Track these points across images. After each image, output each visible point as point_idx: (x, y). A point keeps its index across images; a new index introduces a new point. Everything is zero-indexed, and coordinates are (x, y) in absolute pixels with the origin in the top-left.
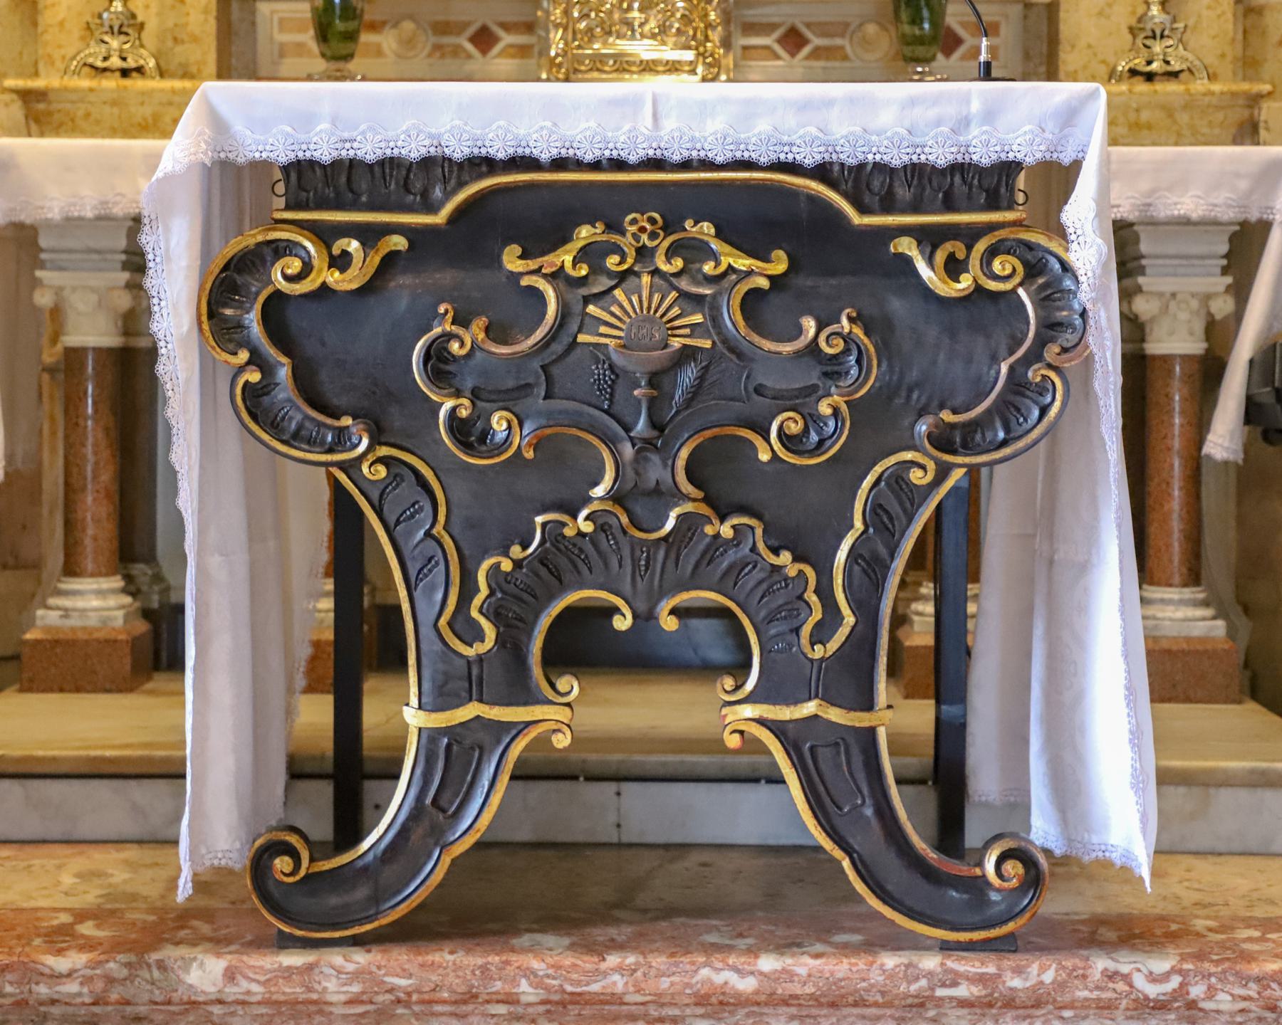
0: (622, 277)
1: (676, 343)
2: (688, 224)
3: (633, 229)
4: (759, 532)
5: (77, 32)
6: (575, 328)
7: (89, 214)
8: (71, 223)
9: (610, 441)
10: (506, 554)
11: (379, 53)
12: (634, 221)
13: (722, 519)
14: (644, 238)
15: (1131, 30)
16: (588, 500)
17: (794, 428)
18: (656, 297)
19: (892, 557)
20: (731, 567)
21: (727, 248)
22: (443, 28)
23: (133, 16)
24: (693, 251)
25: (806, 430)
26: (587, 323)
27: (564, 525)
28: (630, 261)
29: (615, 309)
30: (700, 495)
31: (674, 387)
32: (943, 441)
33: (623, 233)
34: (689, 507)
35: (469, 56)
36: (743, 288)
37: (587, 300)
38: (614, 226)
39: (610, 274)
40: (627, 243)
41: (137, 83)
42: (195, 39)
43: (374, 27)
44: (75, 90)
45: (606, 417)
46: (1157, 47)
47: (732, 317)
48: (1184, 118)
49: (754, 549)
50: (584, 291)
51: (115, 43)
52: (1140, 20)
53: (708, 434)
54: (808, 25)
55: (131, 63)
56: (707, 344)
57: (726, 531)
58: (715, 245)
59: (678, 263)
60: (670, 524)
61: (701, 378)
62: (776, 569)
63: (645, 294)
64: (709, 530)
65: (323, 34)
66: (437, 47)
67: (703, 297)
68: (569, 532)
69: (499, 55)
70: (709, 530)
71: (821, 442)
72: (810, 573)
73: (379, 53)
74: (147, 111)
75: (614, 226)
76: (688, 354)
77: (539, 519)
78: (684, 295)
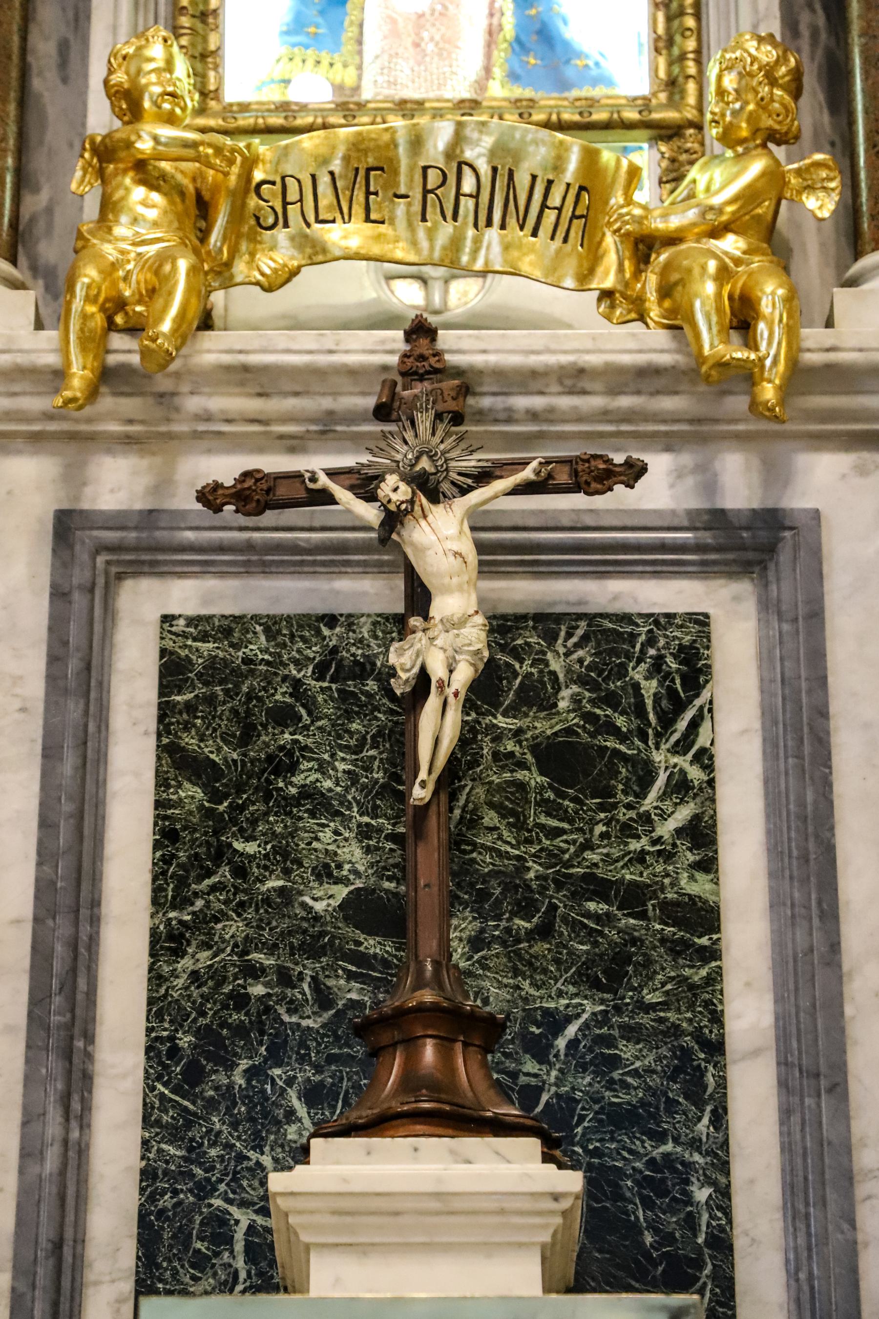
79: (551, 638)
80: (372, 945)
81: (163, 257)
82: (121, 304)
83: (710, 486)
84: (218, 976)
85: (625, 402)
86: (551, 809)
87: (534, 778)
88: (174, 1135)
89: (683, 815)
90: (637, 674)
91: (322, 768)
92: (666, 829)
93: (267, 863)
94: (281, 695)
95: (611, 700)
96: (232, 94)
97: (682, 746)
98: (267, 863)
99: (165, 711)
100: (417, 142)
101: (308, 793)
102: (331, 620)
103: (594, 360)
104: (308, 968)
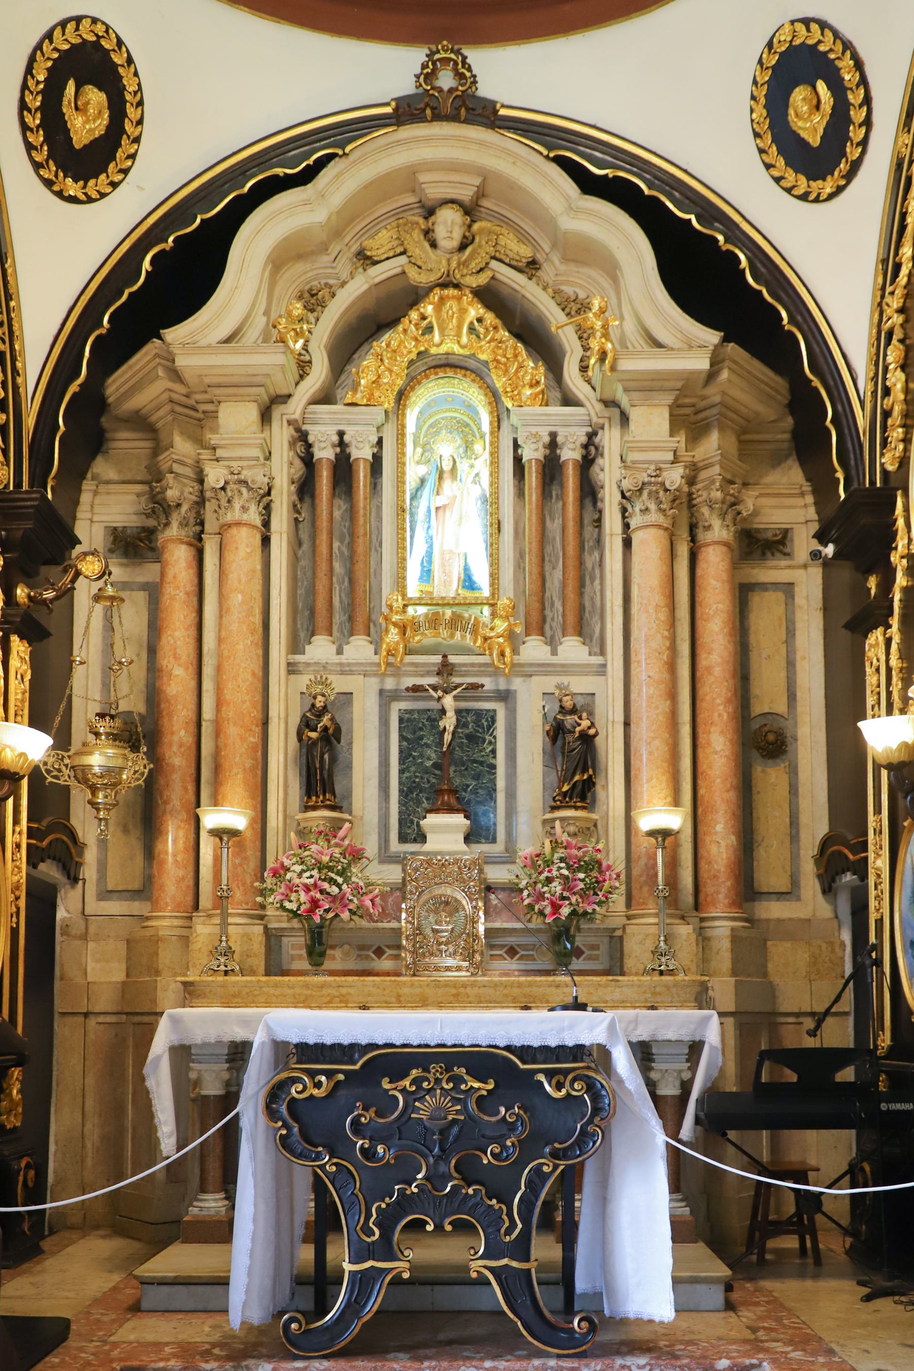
0: (429, 1091)
1: (450, 1117)
2: (455, 1069)
3: (433, 1071)
4: (484, 1192)
5: (206, 953)
6: (410, 1111)
7: (213, 1041)
8: (205, 1045)
9: (425, 1157)
10: (383, 1201)
11: (334, 958)
12: (434, 1068)
13: (469, 1187)
14: (438, 1074)
15: (652, 952)
16: (416, 1179)
17: (497, 1151)
18: (442, 1099)
19: (537, 1201)
20: (472, 1206)
21: (470, 1078)
22: (362, 948)
23: (230, 948)
24: (457, 1080)
25: (501, 1152)
26: (416, 1110)
27: (406, 1189)
28: (432, 1084)
29: (426, 1104)
30: (460, 1177)
31: (449, 1135)
32: (555, 1155)
33: (429, 1072)
34: (456, 1182)
35: (373, 959)
36: (477, 1095)
37: (415, 1100)
38: (426, 1070)
39: (424, 1089)
40: (431, 1077)
41: (231, 979)
42: (256, 955)
43: (333, 947)
44: (206, 982)
45: (423, 1148)
46: (663, 960)
47: (472, 1106)
48: (674, 990)
49: (481, 1198)
50: (414, 1097)
51: (222, 960)
52: (656, 948)
53: (463, 1153)
54: (518, 945)
55: (229, 968)
56: (462, 1118)
57: (471, 1191)
58: (466, 1077)
59: (451, 1085)
60: (448, 1189)
61: (460, 1131)
62: (491, 1206)
63: (438, 1097)
64: (464, 1191)
65: (310, 953)
66: (359, 956)
67: (460, 1099)
68: (408, 1192)
69: (386, 959)
70: (464, 1191)
71: (507, 1156)
72: (504, 1208)
73: (334, 958)
74: (236, 989)
75: (426, 1070)
76: (454, 1121)
77: (397, 1187)
78: (453, 1098)
79: (468, 714)
80: (437, 772)
81: (397, 643)
82: (390, 651)
83: (497, 684)
84: (410, 778)
85: (482, 669)
86: (468, 747)
87: (465, 741)
88: (404, 805)
89: (490, 748)
90: (483, 721)
91: (428, 739)
92: (488, 750)
93: (418, 757)
94: (420, 725)
95: (478, 726)
96: (409, 595)
97: (491, 735)
98: (418, 757)
99: (400, 728)
100: (444, 614)
101: (425, 744)
102: (429, 710)
103: (476, 662)
104: (426, 776)
